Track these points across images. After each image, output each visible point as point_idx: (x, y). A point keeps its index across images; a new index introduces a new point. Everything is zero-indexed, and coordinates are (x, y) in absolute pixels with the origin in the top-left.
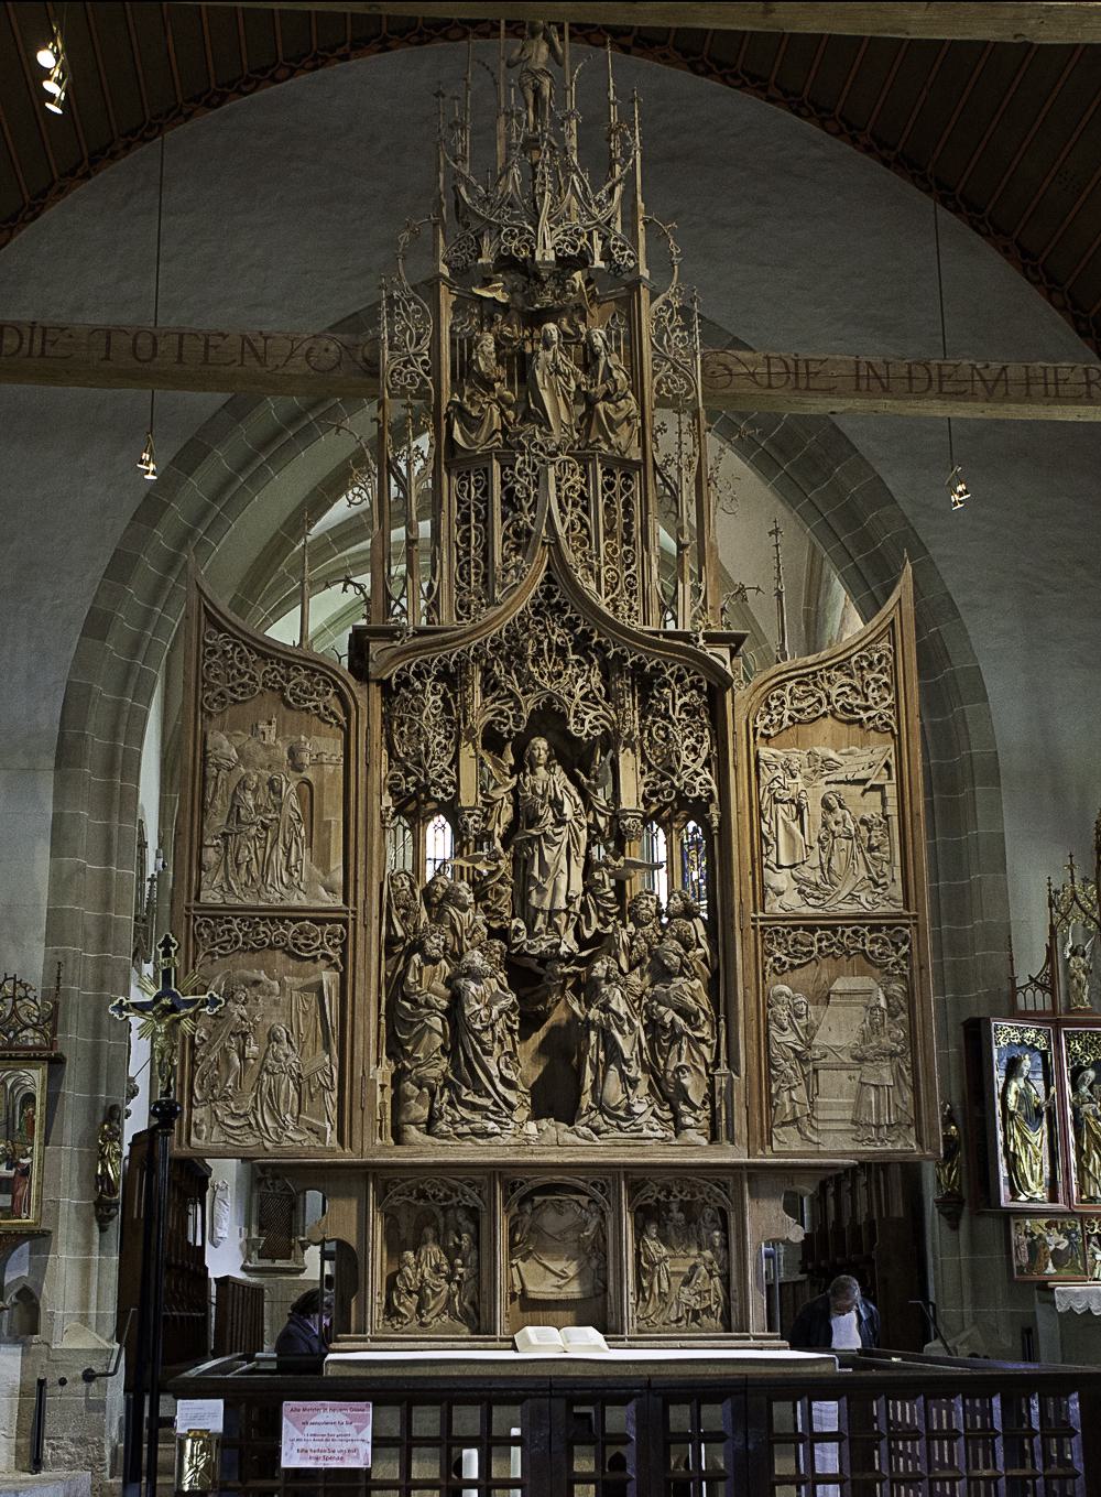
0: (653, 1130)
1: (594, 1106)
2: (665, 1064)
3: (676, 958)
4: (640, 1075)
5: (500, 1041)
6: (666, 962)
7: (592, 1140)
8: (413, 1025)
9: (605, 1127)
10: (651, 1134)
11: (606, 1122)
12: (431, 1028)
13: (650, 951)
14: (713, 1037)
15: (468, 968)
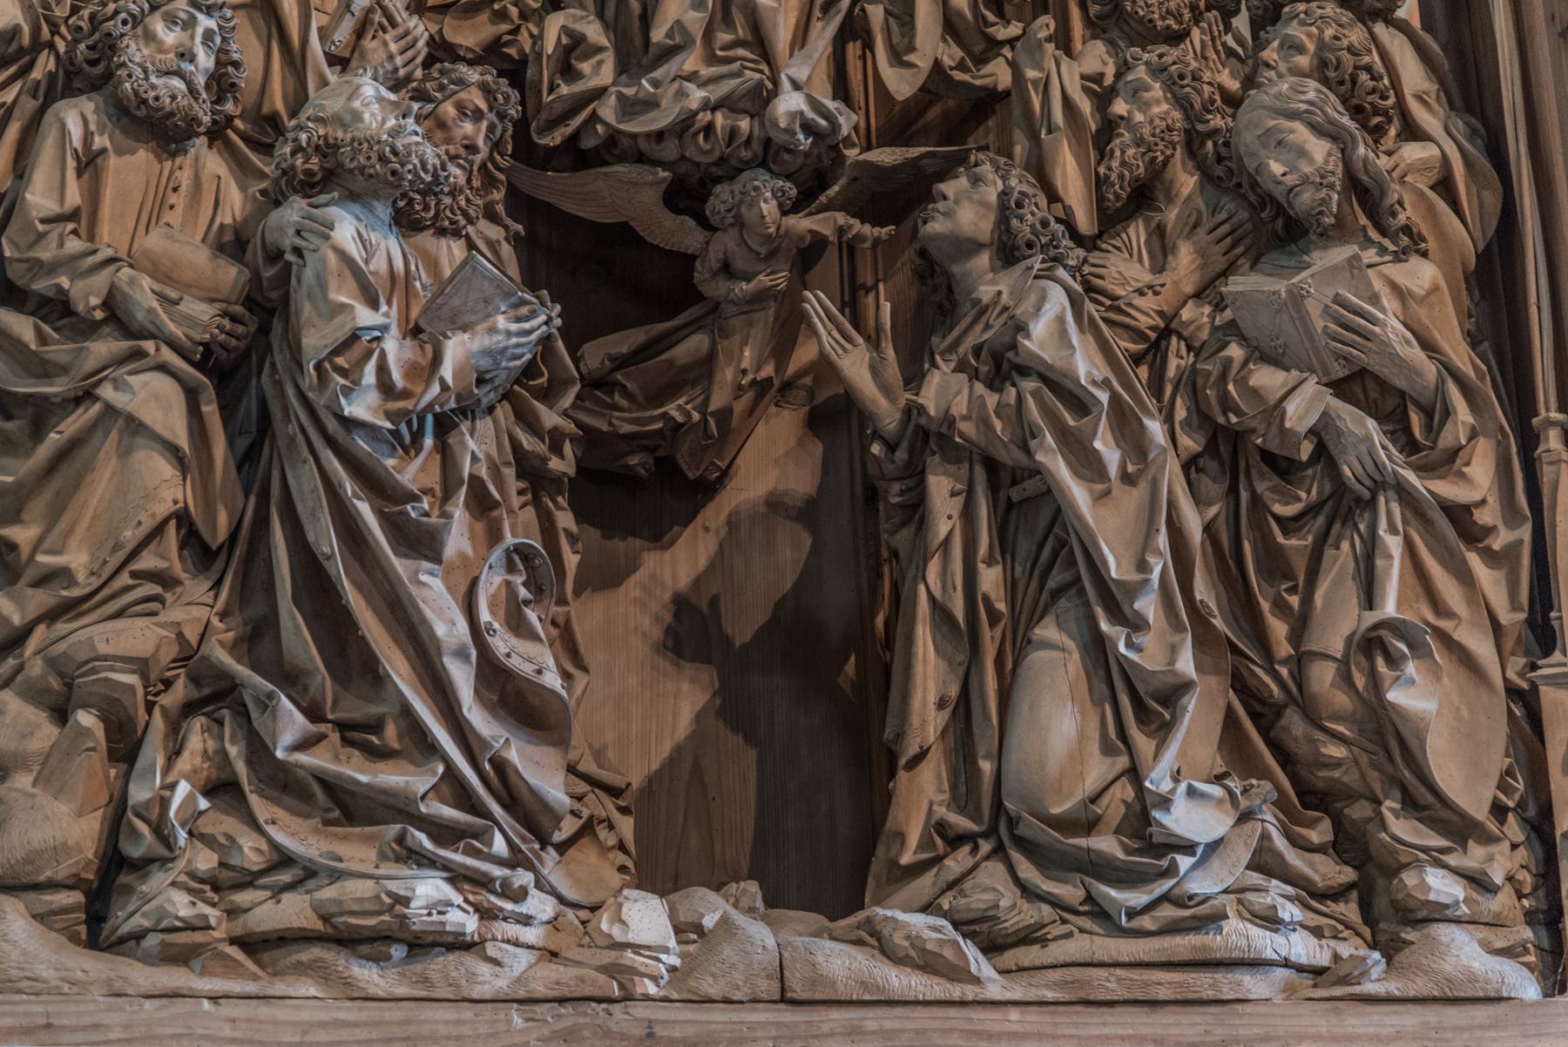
0: (1270, 921)
1: (963, 823)
2: (1296, 637)
3: (1319, 149)
4: (1186, 664)
5: (481, 504)
6: (1276, 168)
7: (959, 973)
8: (41, 414)
9: (1030, 914)
10: (1266, 942)
11: (1028, 892)
12: (134, 426)
13: (1193, 141)
14: (1511, 515)
15: (327, 149)
